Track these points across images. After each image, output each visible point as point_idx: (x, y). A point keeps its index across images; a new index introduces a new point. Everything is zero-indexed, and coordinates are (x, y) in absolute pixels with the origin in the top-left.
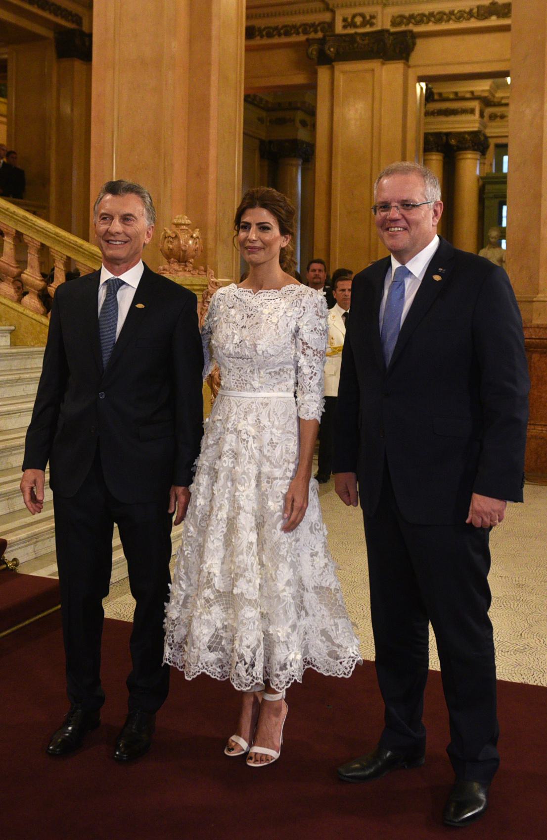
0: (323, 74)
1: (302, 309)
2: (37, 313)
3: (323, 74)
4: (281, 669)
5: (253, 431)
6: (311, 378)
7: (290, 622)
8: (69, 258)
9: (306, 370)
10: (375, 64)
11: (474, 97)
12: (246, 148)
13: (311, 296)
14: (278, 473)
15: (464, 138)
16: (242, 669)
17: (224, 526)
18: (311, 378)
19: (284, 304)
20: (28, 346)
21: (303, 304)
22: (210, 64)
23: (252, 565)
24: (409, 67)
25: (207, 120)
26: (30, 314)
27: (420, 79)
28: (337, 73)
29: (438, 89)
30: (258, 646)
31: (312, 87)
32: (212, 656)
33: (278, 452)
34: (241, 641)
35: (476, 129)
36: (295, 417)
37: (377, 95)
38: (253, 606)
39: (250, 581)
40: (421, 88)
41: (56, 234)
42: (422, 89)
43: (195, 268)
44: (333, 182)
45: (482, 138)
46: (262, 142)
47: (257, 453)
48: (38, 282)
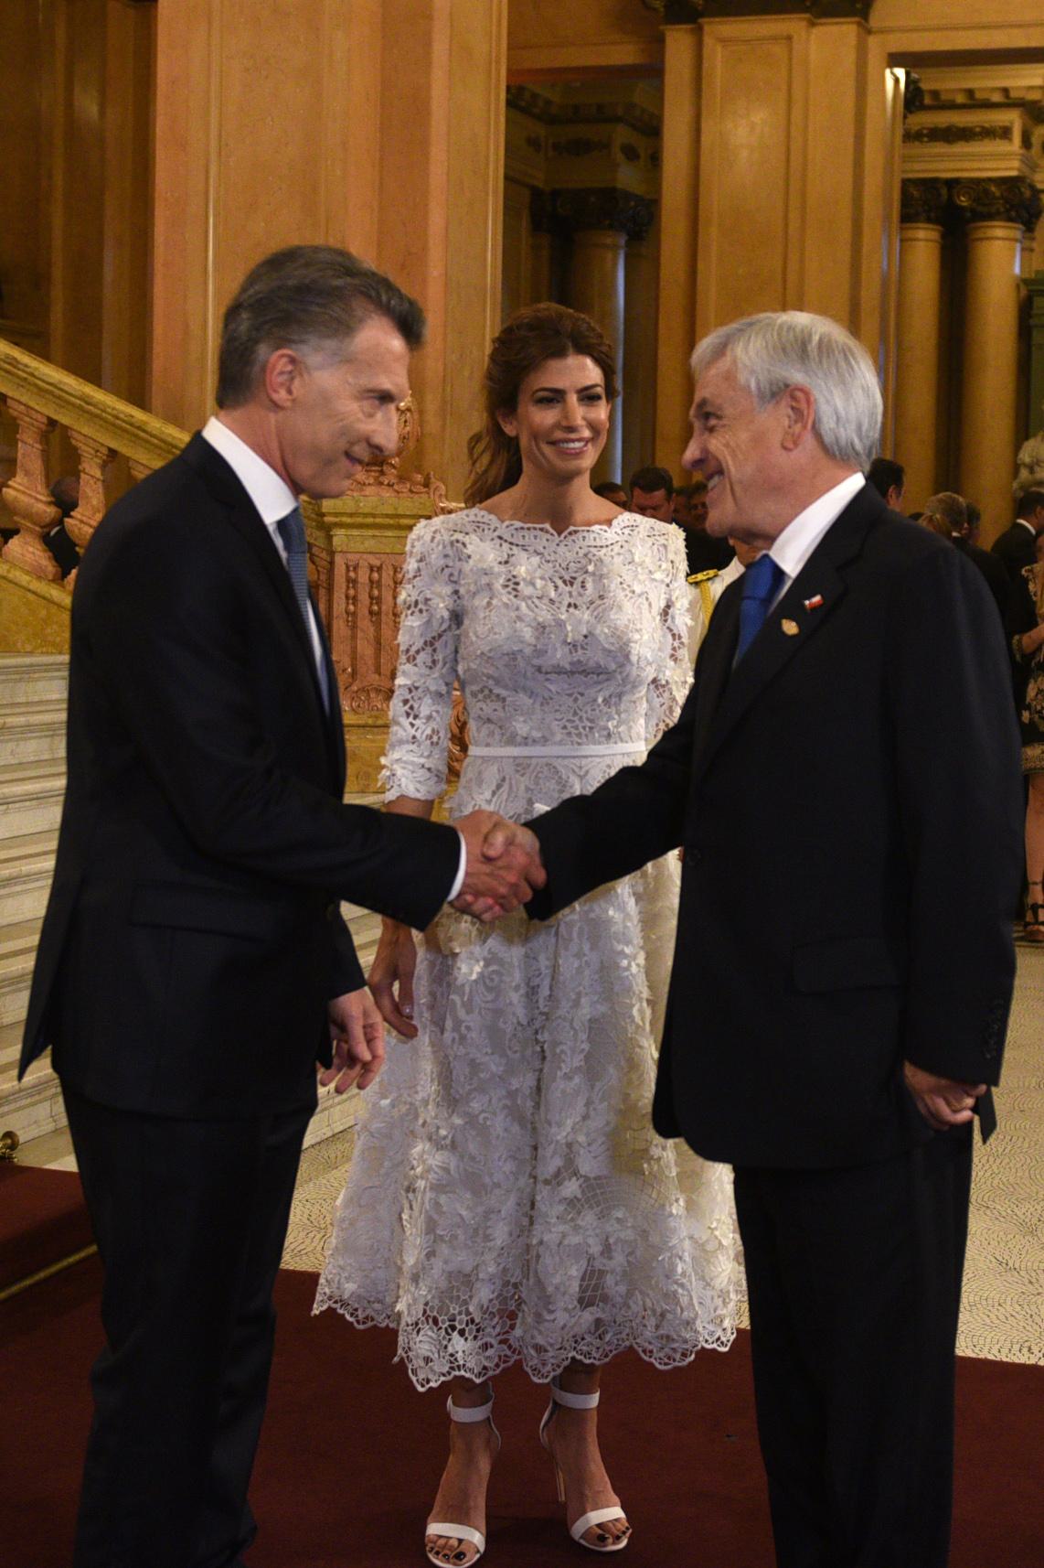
0: (678, 42)
2: (39, 578)
3: (678, 42)
8: (113, 453)
10: (793, 25)
11: (1009, 102)
12: (509, 210)
15: (986, 192)
20: (18, 653)
22: (430, 18)
24: (869, 32)
25: (424, 144)
26: (24, 579)
27: (895, 60)
28: (708, 41)
29: (933, 81)
31: (654, 71)
35: (1014, 173)
37: (798, 93)
40: (894, 79)
41: (86, 399)
42: (897, 80)
43: (402, 479)
44: (700, 288)
45: (1028, 193)
46: (536, 193)
48: (41, 507)
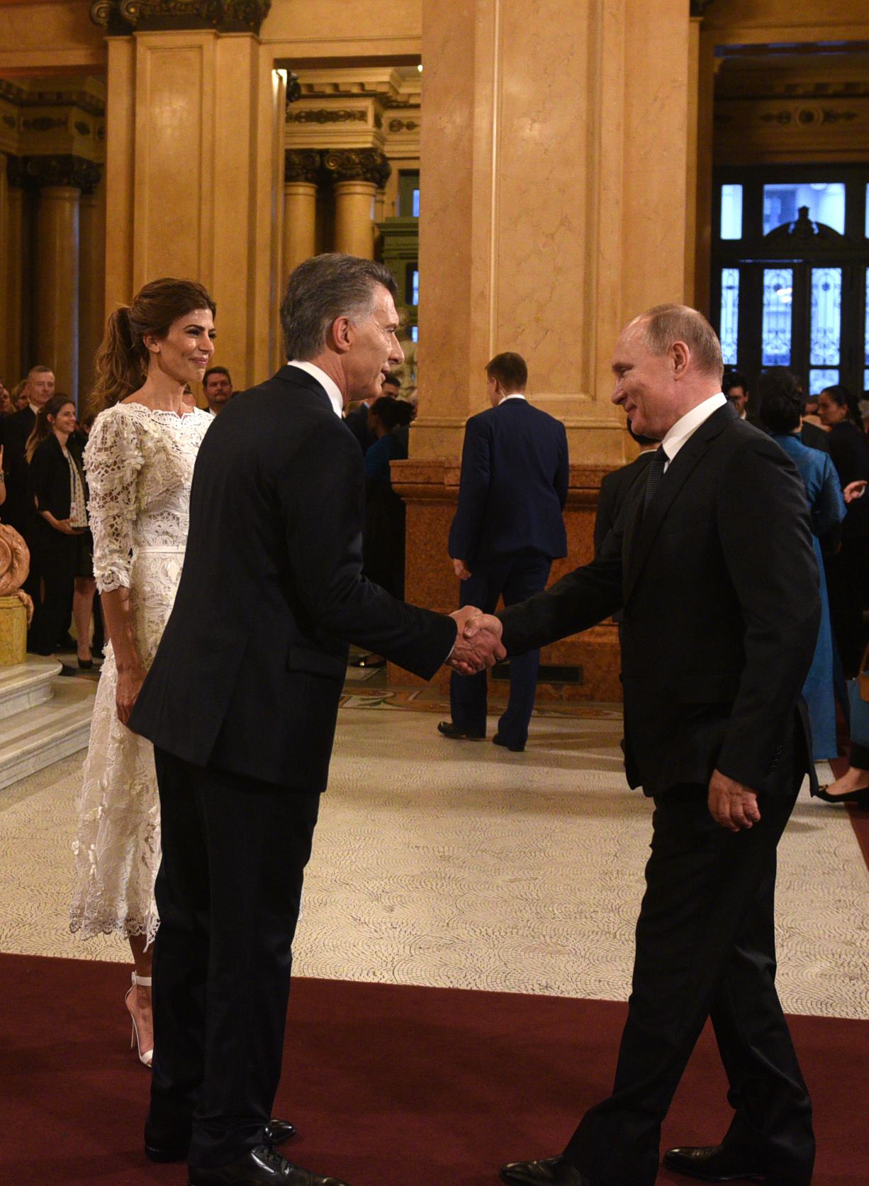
0: (118, 50)
3: (118, 50)
10: (203, 37)
11: (365, 93)
15: (348, 159)
24: (260, 43)
27: (279, 63)
28: (140, 49)
29: (305, 78)
31: (100, 70)
35: (369, 146)
37: (208, 89)
40: (279, 78)
42: (281, 78)
45: (379, 161)
46: (11, 158)
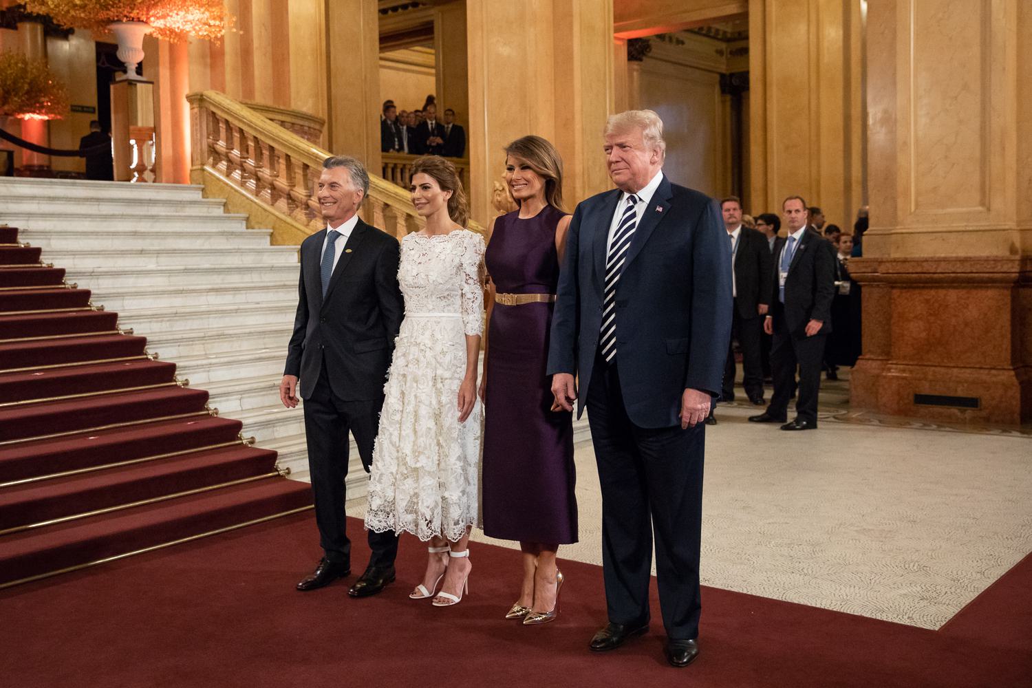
1: (464, 249)
4: (455, 524)
5: (429, 344)
6: (473, 302)
7: (461, 489)
9: (469, 295)
13: (471, 238)
14: (447, 374)
16: (423, 524)
17: (412, 417)
18: (473, 302)
19: (449, 246)
21: (465, 245)
23: (430, 444)
30: (436, 506)
32: (410, 517)
33: (448, 358)
34: (423, 503)
36: (462, 332)
38: (431, 476)
39: (428, 458)
41: (396, 194)
47: (433, 362)
